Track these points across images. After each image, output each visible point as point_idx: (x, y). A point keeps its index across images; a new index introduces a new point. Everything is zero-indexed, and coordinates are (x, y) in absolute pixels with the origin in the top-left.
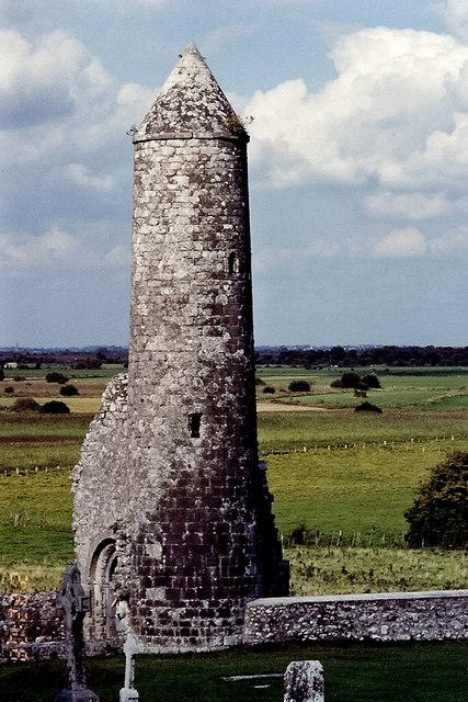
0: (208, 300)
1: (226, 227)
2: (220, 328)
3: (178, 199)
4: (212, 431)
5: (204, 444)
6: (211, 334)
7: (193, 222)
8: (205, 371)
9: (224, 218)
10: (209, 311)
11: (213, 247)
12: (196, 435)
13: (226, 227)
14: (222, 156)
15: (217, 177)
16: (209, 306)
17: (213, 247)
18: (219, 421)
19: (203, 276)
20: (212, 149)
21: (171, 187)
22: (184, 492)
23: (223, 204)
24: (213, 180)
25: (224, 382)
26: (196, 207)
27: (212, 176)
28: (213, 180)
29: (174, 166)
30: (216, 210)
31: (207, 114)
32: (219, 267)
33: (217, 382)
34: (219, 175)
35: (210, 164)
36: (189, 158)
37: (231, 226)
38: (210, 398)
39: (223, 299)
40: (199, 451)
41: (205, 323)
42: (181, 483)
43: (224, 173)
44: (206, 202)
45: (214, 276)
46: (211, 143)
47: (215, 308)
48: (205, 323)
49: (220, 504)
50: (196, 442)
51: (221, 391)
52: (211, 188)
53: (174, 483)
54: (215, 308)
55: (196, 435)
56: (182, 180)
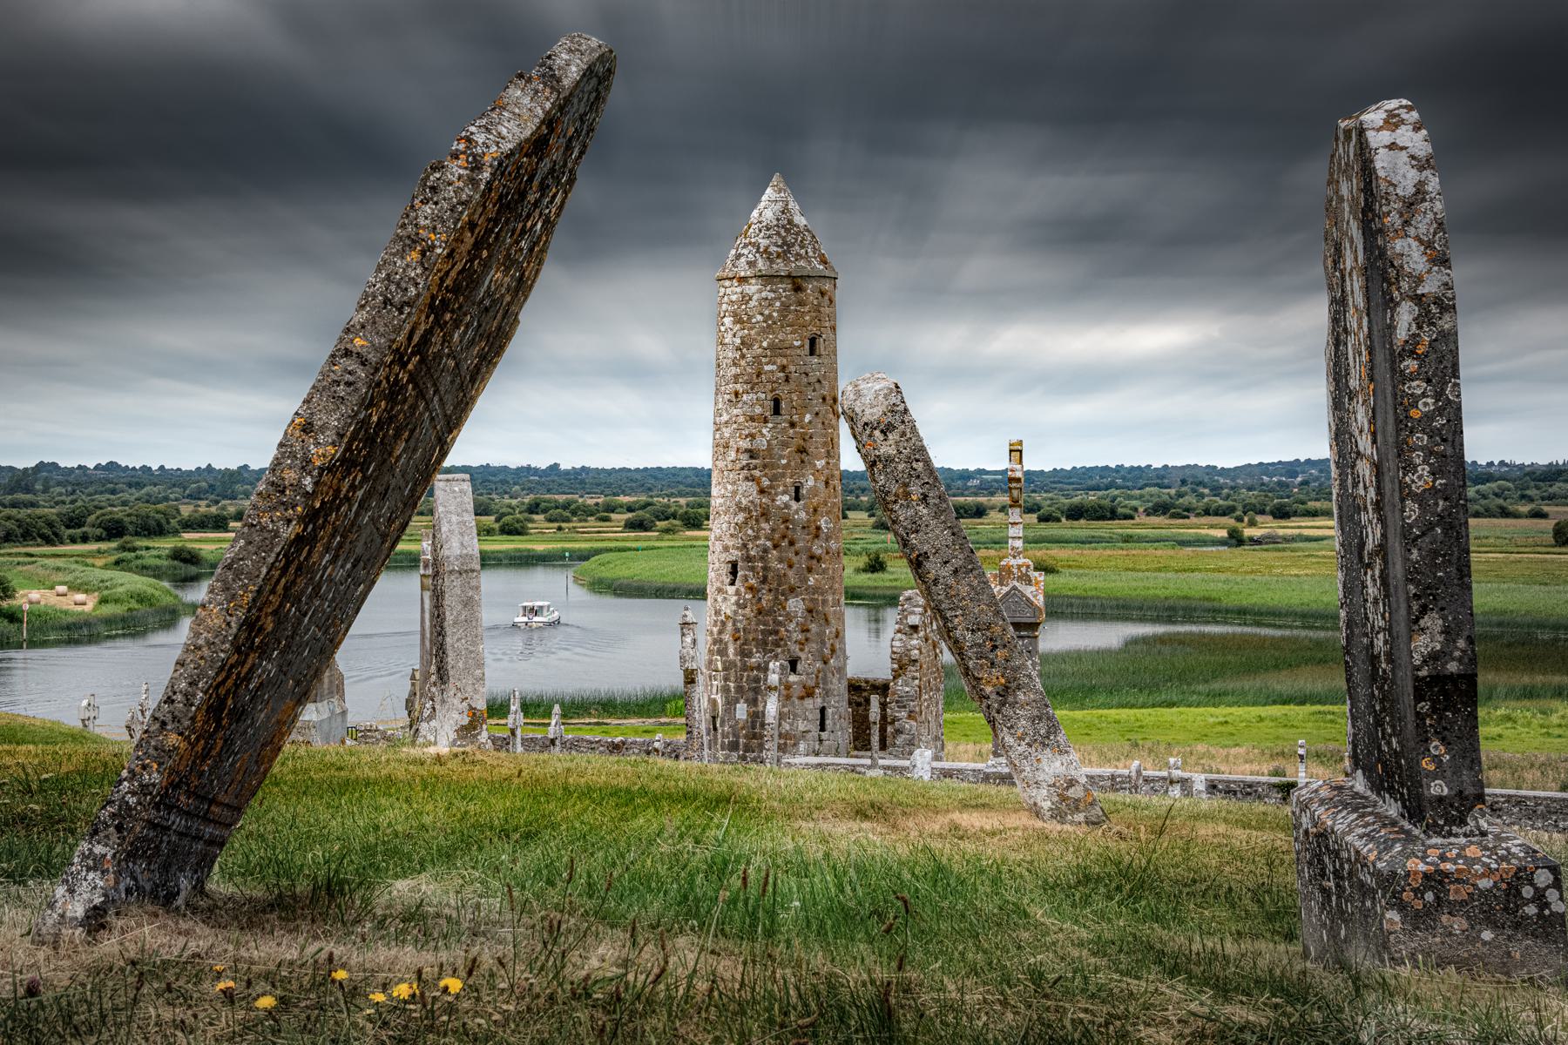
0: (745, 444)
1: (767, 368)
2: (757, 473)
3: (726, 341)
4: (746, 578)
5: (737, 593)
6: (747, 479)
7: (735, 364)
8: (741, 517)
9: (764, 360)
10: (746, 456)
11: (752, 389)
12: (732, 583)
13: (767, 368)
14: (764, 294)
15: (760, 318)
16: (747, 451)
17: (752, 389)
18: (752, 569)
19: (741, 419)
20: (752, 288)
21: (723, 329)
22: (721, 641)
23: (765, 344)
24: (754, 320)
25: (759, 529)
26: (738, 349)
27: (754, 316)
28: (754, 320)
29: (724, 307)
30: (757, 350)
31: (758, 251)
32: (758, 410)
33: (752, 528)
34: (762, 314)
35: (752, 303)
36: (734, 298)
37: (775, 367)
38: (745, 546)
39: (761, 443)
40: (734, 599)
41: (742, 469)
42: (720, 632)
43: (767, 312)
44: (746, 343)
45: (752, 419)
46: (753, 281)
47: (752, 454)
48: (742, 469)
49: (750, 655)
50: (731, 590)
51: (757, 538)
52: (752, 329)
53: (715, 630)
54: (752, 454)
55: (732, 583)
56: (728, 321)
